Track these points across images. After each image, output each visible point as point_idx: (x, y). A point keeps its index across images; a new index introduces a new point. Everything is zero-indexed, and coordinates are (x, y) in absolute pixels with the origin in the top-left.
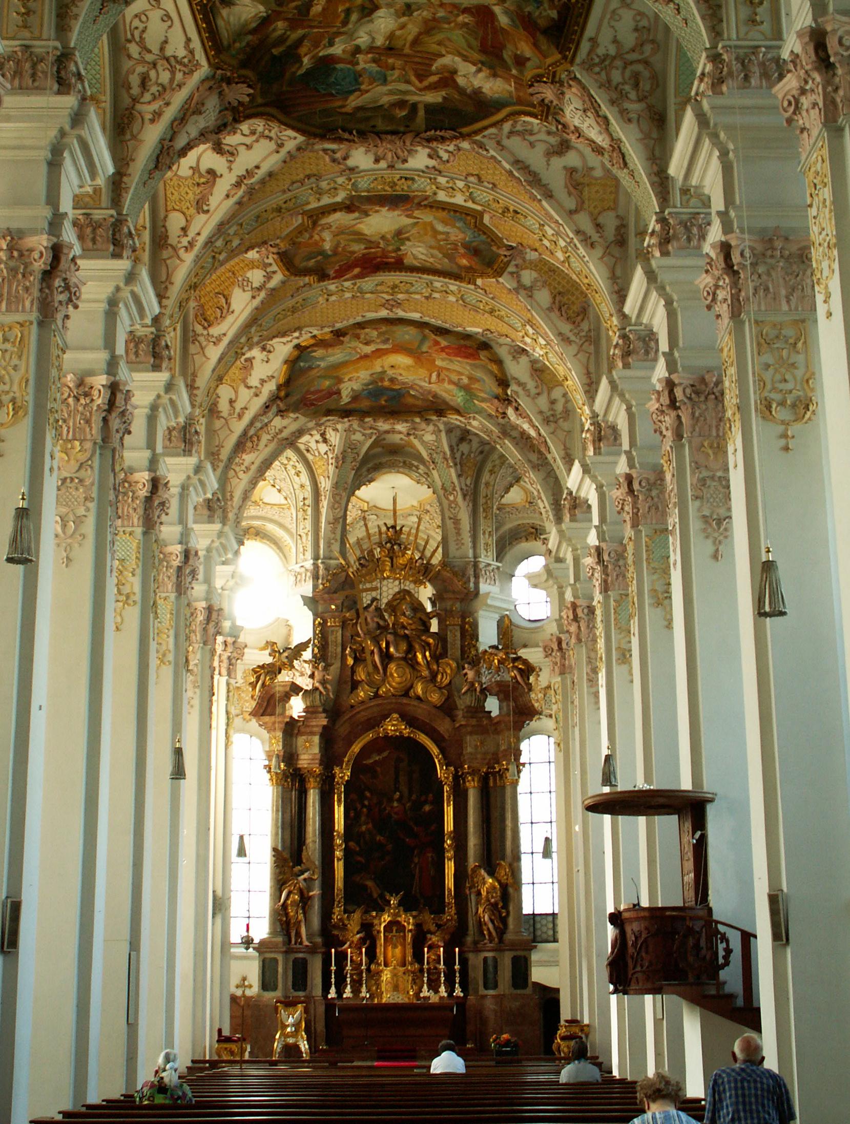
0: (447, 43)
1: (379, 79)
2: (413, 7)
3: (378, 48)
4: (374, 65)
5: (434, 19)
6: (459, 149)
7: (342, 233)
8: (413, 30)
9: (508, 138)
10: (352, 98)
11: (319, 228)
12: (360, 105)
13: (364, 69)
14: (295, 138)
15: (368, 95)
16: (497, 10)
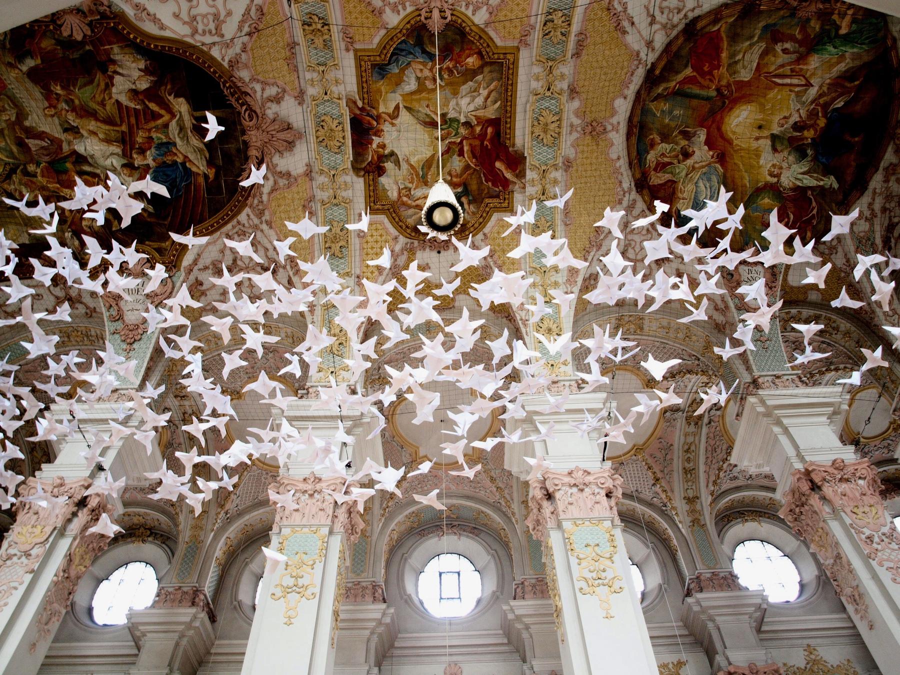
0: (99, 98)
1: (168, 148)
2: (66, 126)
3: (123, 151)
4: (148, 153)
5: (74, 110)
6: (253, 79)
7: (424, 176)
8: (93, 125)
9: (222, 36)
10: (194, 169)
11: (405, 199)
12: (205, 163)
13: (154, 160)
14: (248, 215)
15: (191, 157)
16: (25, 68)
